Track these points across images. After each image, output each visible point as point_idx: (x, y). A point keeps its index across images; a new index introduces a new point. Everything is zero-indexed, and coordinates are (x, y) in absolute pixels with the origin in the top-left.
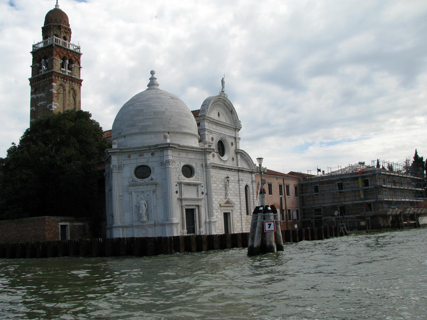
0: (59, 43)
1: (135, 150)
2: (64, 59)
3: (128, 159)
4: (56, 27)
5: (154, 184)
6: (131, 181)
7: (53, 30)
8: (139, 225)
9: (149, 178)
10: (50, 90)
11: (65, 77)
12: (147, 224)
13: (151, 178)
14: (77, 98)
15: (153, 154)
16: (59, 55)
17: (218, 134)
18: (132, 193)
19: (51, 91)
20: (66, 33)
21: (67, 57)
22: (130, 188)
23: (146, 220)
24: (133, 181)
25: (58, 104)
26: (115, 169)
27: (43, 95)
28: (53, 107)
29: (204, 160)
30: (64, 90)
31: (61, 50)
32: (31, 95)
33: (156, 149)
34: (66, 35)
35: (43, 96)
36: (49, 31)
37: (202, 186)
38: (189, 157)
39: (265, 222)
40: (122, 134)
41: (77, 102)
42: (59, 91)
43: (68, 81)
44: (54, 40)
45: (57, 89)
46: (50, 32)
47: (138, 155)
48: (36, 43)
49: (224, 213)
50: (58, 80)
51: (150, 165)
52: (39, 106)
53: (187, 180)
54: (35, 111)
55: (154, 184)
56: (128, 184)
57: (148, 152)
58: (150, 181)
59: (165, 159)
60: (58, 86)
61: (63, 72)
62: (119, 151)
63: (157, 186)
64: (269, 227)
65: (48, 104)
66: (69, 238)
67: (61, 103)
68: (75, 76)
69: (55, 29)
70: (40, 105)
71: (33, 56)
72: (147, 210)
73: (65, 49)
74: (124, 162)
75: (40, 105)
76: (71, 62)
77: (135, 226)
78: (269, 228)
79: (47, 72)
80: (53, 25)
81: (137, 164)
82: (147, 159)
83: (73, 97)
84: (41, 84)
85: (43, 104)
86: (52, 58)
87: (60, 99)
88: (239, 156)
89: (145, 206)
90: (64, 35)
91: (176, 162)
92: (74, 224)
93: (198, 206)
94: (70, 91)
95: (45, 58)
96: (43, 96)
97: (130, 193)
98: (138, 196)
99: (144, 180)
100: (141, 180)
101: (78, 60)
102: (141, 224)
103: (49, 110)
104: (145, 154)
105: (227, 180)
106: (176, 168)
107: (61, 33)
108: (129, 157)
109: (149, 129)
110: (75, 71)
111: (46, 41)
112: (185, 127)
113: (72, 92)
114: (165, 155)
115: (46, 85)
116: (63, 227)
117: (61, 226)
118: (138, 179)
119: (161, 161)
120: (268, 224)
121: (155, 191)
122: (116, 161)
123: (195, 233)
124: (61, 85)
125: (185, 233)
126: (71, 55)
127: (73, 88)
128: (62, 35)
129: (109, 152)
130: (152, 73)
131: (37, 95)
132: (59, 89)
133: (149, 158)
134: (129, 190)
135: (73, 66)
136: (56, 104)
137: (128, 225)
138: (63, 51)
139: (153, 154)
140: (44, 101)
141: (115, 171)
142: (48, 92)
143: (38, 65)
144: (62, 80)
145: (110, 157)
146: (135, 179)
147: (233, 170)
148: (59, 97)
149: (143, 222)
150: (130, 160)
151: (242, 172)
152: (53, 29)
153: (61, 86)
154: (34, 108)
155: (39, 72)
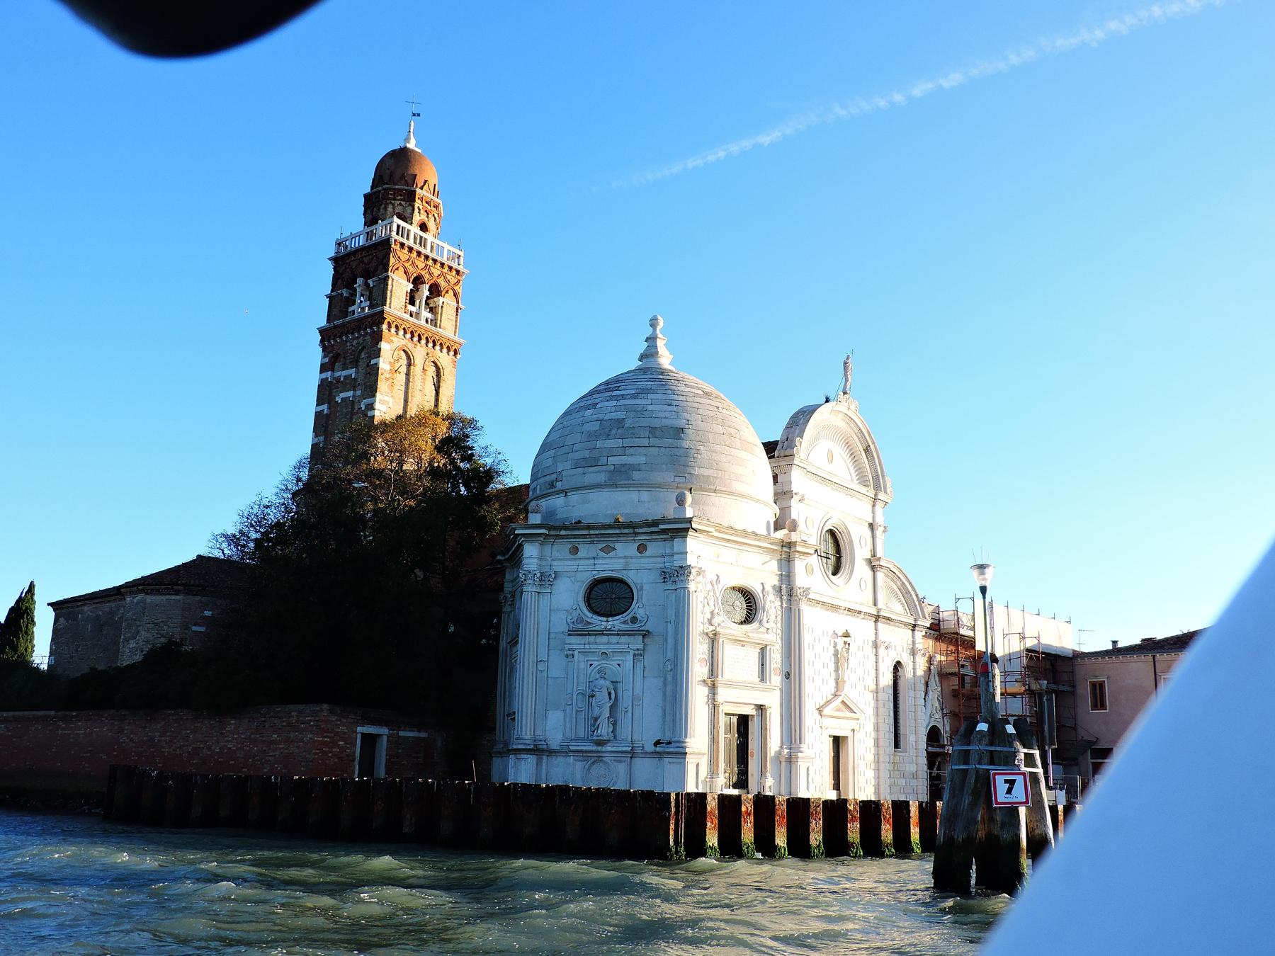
0: (408, 239)
1: (592, 532)
2: (418, 281)
3: (572, 557)
4: (401, 195)
5: (641, 634)
6: (574, 620)
7: (393, 202)
8: (586, 752)
9: (627, 616)
10: (373, 362)
12: (609, 749)
13: (630, 616)
14: (444, 388)
15: (642, 548)
16: (405, 268)
23: (608, 738)
24: (580, 620)
25: (391, 400)
26: (529, 581)
27: (352, 372)
28: (377, 406)
29: (785, 576)
32: (321, 372)
33: (652, 533)
36: (383, 206)
39: (994, 775)
40: (559, 485)
44: (395, 228)
46: (386, 209)
47: (601, 546)
48: (346, 234)
51: (631, 577)
54: (327, 414)
55: (641, 634)
56: (565, 628)
57: (626, 542)
58: (628, 623)
59: (677, 564)
61: (411, 315)
62: (547, 532)
63: (647, 640)
64: (1009, 791)
65: (365, 399)
66: (381, 772)
69: (398, 200)
71: (335, 269)
72: (613, 708)
74: (558, 566)
76: (435, 290)
77: (574, 751)
78: (1007, 793)
80: (394, 189)
81: (594, 572)
82: (622, 561)
84: (348, 344)
86: (385, 274)
87: (396, 388)
89: (610, 694)
92: (402, 734)
95: (367, 276)
97: (567, 656)
98: (591, 665)
99: (610, 619)
100: (605, 619)
102: (594, 748)
103: (366, 415)
104: (617, 546)
105: (845, 643)
108: (575, 550)
113: (431, 371)
114: (678, 553)
115: (364, 347)
116: (370, 741)
117: (364, 735)
118: (595, 617)
119: (665, 570)
120: (1006, 781)
121: (641, 655)
122: (536, 561)
123: (747, 787)
125: (722, 785)
126: (436, 272)
129: (517, 532)
131: (337, 374)
133: (631, 557)
134: (567, 647)
135: (441, 299)
136: (386, 398)
139: (642, 548)
140: (355, 390)
141: (530, 589)
143: (345, 293)
145: (520, 546)
146: (585, 615)
147: (862, 616)
148: (394, 381)
149: (600, 743)
150: (575, 559)
151: (887, 623)
152: (395, 200)
155: (347, 311)
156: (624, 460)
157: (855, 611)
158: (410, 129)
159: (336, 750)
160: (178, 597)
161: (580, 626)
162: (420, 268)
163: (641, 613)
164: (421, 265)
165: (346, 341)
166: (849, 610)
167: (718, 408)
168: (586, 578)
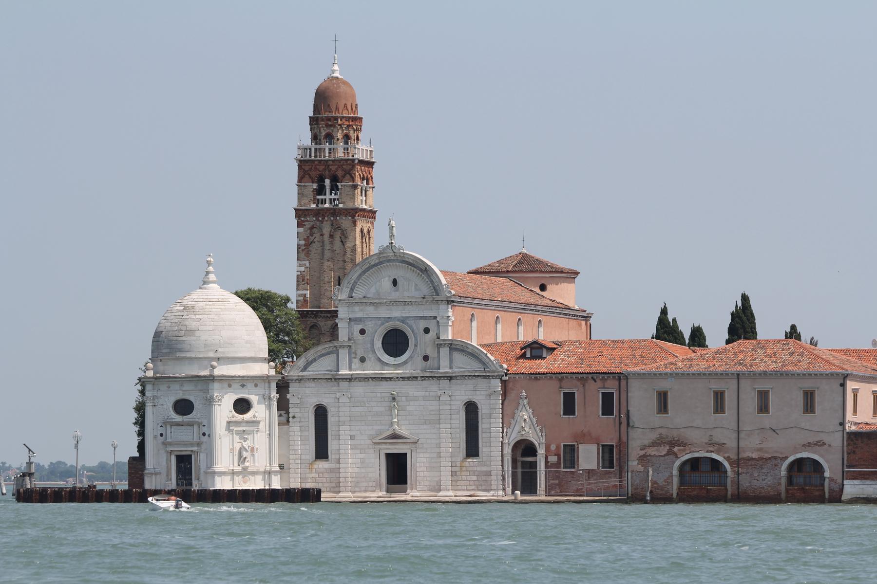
11: (318, 213)
16: (309, 175)
17: (383, 319)
20: (331, 126)
21: (327, 173)
30: (322, 235)
31: (312, 166)
34: (331, 131)
37: (204, 426)
38: (184, 389)
41: (349, 250)
42: (312, 238)
43: (326, 218)
45: (306, 238)
49: (388, 456)
50: (307, 221)
53: (178, 418)
60: (306, 231)
67: (316, 259)
68: (343, 203)
73: (320, 161)
76: (335, 180)
83: (342, 242)
88: (445, 351)
90: (327, 131)
91: (162, 397)
93: (192, 451)
94: (332, 233)
101: (351, 172)
105: (394, 399)
106: (162, 405)
107: (320, 130)
110: (342, 194)
112: (180, 350)
113: (338, 235)
124: (312, 228)
126: (333, 168)
127: (338, 227)
128: (324, 134)
132: (312, 236)
138: (317, 167)
144: (314, 219)
147: (419, 379)
153: (315, 229)
157: (410, 377)
158: (335, 61)
159: (138, 475)
162: (320, 170)
164: (321, 168)
166: (401, 377)
167: (183, 316)
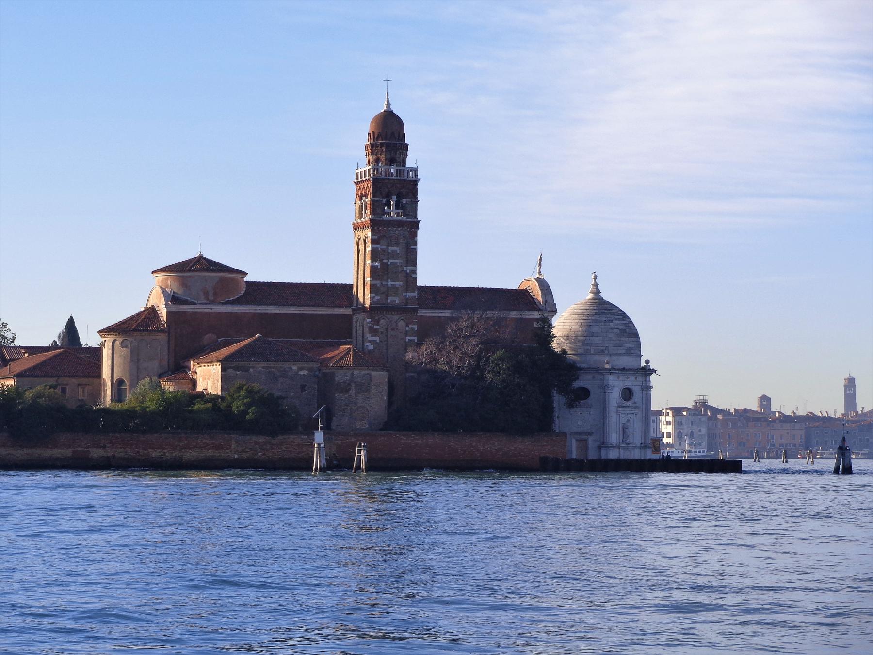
10: (412, 247)
15: (636, 378)
18: (620, 415)
19: (415, 249)
22: (619, 409)
24: (620, 402)
27: (398, 250)
35: (398, 252)
40: (607, 351)
52: (389, 264)
70: (391, 263)
75: (391, 263)
79: (404, 218)
84: (392, 232)
85: (397, 263)
96: (398, 252)
102: (626, 446)
104: (629, 377)
108: (619, 378)
109: (633, 351)
111: (400, 170)
130: (596, 278)
137: (615, 445)
139: (636, 378)
142: (408, 248)
154: (377, 264)
156: (630, 346)
160: (382, 373)
161: (620, 404)
163: (636, 401)
165: (390, 230)
168: (622, 387)
